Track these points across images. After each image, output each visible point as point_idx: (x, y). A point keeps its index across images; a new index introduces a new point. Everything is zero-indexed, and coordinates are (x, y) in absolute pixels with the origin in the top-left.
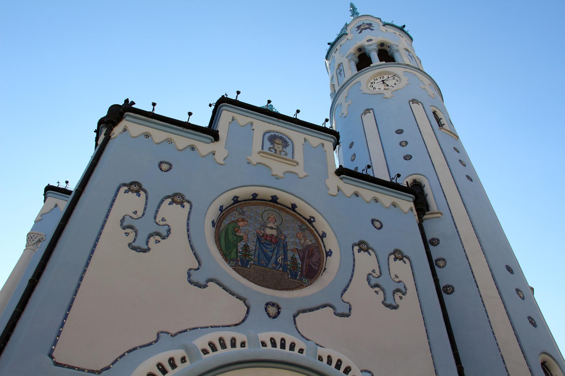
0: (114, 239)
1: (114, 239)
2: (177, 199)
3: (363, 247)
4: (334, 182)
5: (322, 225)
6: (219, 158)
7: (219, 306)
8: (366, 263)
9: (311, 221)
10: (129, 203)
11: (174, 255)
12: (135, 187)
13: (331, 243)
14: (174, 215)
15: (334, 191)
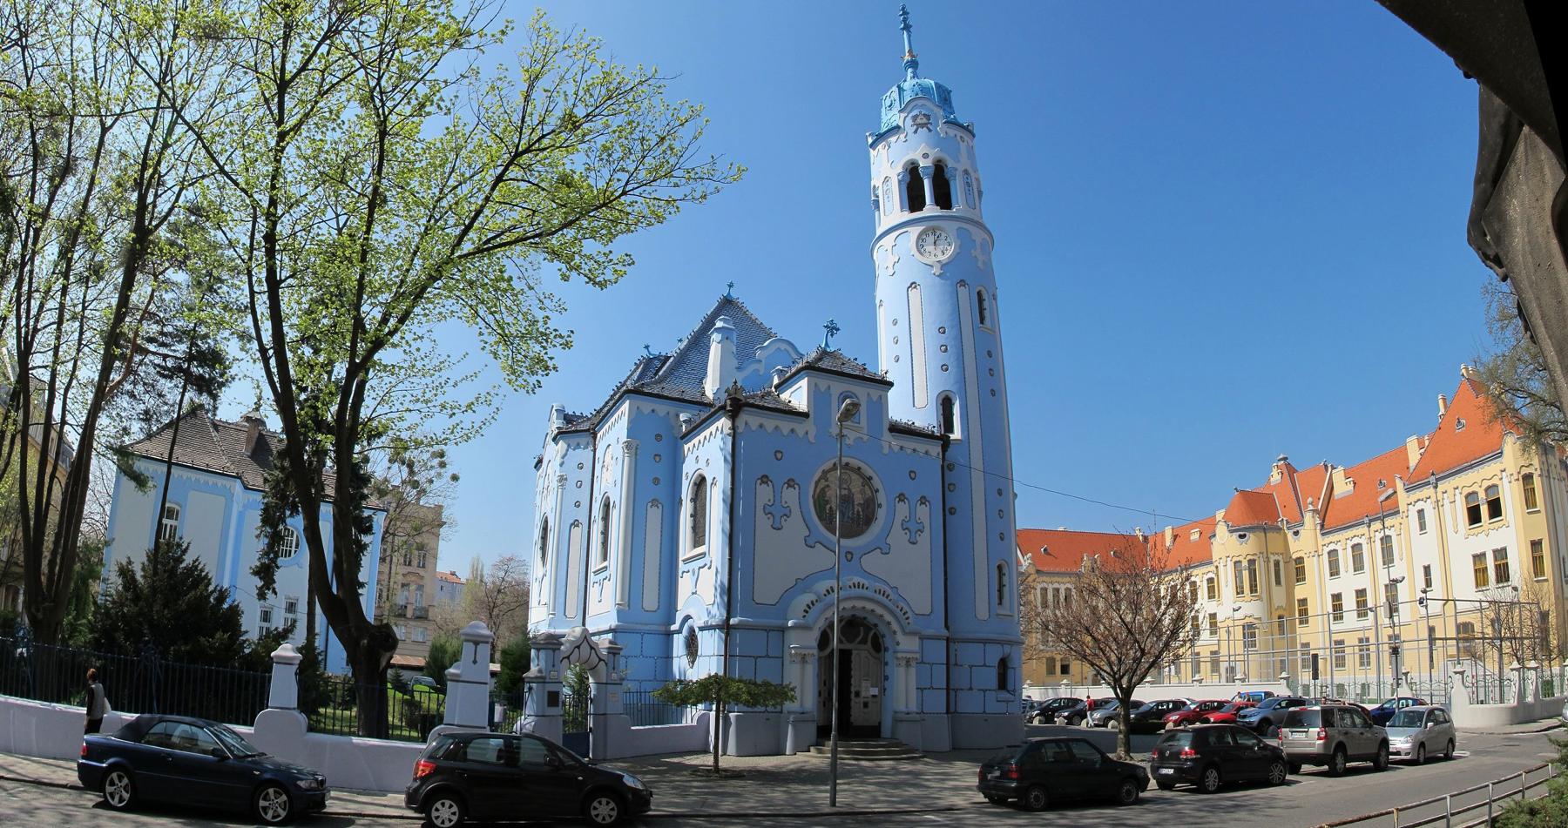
0: (763, 522)
1: (763, 522)
2: (790, 483)
3: (902, 498)
4: (887, 436)
5: (876, 483)
6: (811, 437)
7: (824, 559)
8: (902, 510)
9: (870, 478)
10: (765, 493)
11: (795, 528)
12: (765, 479)
13: (881, 498)
14: (790, 496)
15: (886, 451)
